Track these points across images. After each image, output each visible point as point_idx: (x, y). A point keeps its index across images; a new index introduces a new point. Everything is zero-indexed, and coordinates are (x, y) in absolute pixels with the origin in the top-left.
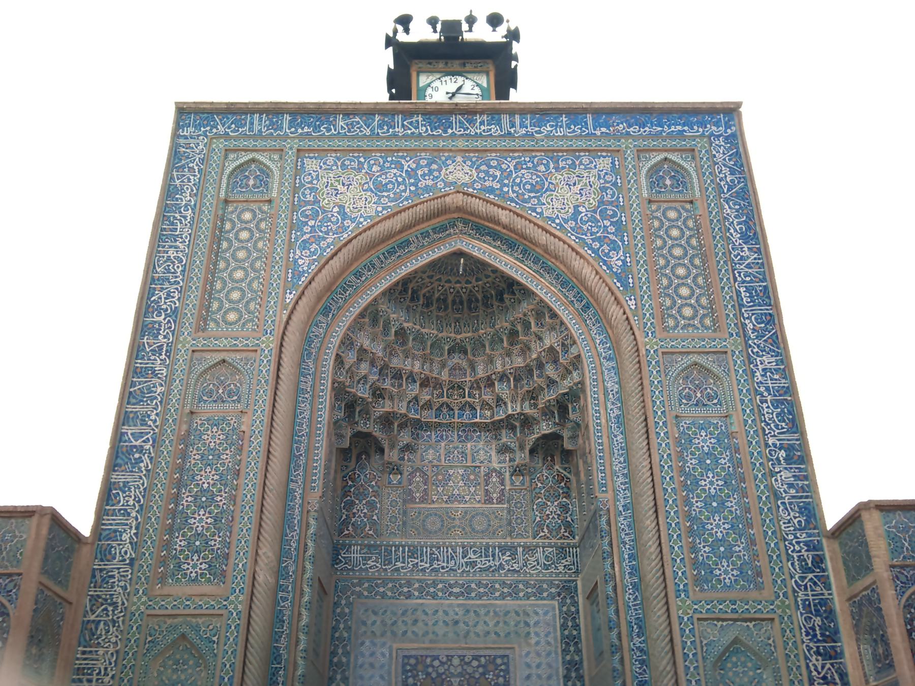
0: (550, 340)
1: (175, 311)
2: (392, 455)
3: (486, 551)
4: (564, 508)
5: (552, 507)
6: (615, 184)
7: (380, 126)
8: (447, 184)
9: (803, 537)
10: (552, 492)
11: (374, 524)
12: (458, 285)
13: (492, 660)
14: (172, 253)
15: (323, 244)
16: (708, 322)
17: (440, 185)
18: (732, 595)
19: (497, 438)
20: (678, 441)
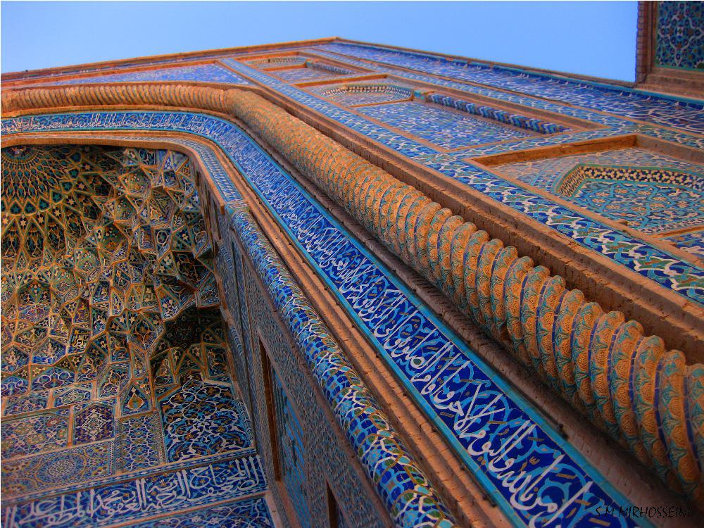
10: (199, 407)
12: (30, 215)
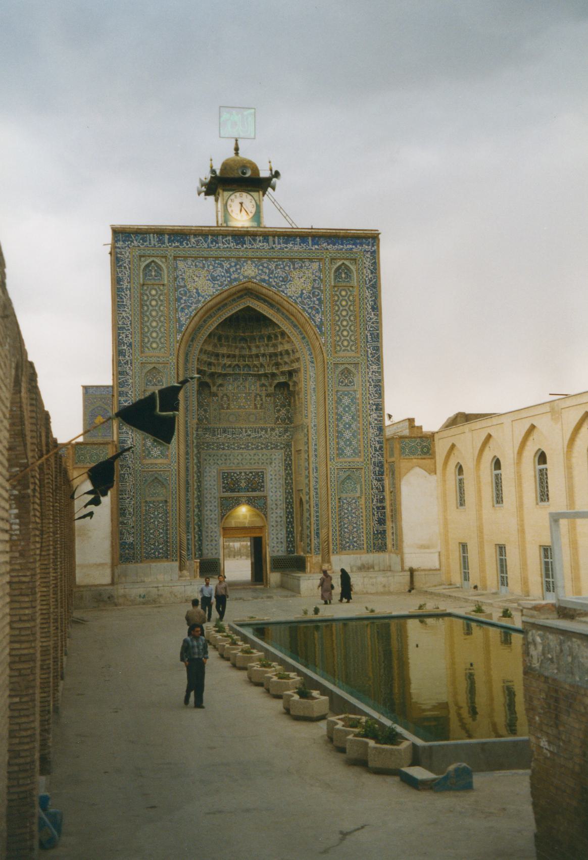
0: (287, 347)
1: (130, 344)
2: (214, 389)
3: (255, 430)
4: (288, 411)
5: (283, 411)
6: (320, 278)
7: (212, 242)
8: (245, 277)
9: (377, 439)
11: (207, 419)
13: (257, 473)
14: (124, 314)
15: (191, 309)
16: (353, 348)
17: (241, 277)
18: (349, 460)
19: (260, 380)
20: (336, 402)
